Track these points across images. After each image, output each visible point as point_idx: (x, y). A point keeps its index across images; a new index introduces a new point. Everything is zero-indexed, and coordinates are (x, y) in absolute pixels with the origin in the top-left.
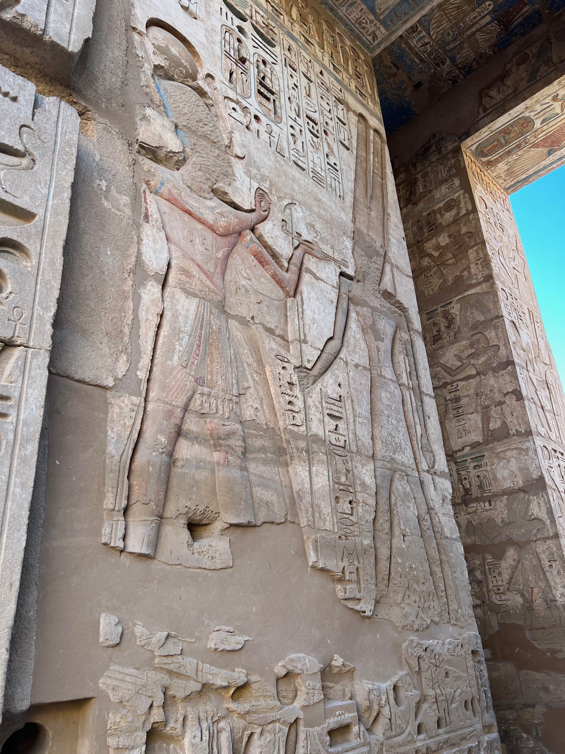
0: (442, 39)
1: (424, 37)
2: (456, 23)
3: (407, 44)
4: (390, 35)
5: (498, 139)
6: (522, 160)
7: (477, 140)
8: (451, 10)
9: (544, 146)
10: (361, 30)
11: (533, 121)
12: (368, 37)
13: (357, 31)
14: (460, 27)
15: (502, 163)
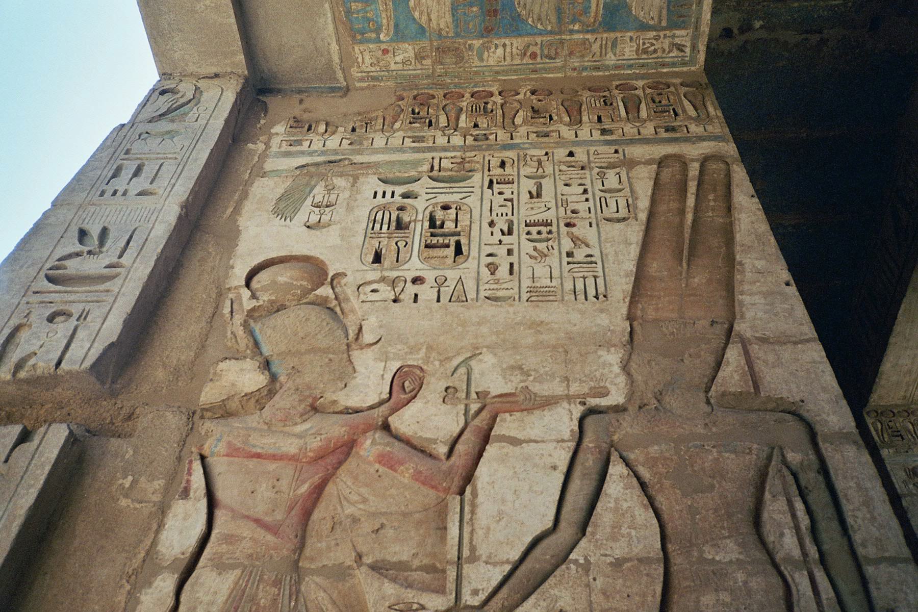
4: (697, 28)
10: (654, 56)
12: (671, 55)
13: (650, 61)
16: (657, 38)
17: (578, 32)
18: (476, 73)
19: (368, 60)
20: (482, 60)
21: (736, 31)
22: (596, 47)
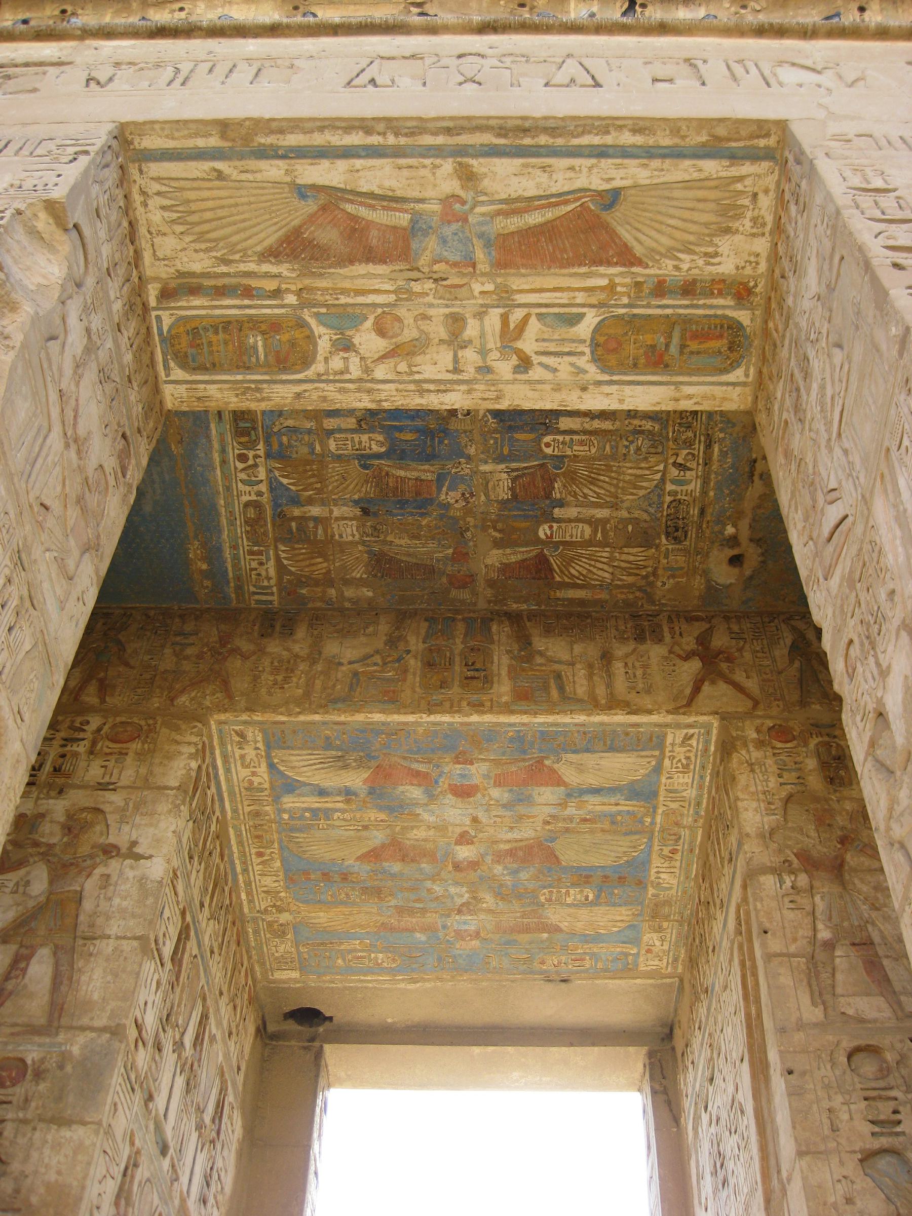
0: (653, 450)
1: (673, 482)
2: (615, 459)
3: (704, 492)
4: (667, 725)
5: (682, 353)
6: (678, 234)
7: (718, 391)
8: (605, 485)
9: (613, 234)
10: (693, 759)
11: (592, 339)
12: (695, 744)
14: (612, 448)
15: (720, 269)
16: (672, 758)
17: (653, 818)
18: (684, 892)
19: (657, 963)
20: (671, 888)
21: (736, 552)
22: (673, 805)
